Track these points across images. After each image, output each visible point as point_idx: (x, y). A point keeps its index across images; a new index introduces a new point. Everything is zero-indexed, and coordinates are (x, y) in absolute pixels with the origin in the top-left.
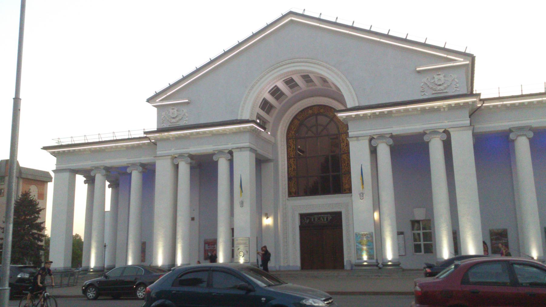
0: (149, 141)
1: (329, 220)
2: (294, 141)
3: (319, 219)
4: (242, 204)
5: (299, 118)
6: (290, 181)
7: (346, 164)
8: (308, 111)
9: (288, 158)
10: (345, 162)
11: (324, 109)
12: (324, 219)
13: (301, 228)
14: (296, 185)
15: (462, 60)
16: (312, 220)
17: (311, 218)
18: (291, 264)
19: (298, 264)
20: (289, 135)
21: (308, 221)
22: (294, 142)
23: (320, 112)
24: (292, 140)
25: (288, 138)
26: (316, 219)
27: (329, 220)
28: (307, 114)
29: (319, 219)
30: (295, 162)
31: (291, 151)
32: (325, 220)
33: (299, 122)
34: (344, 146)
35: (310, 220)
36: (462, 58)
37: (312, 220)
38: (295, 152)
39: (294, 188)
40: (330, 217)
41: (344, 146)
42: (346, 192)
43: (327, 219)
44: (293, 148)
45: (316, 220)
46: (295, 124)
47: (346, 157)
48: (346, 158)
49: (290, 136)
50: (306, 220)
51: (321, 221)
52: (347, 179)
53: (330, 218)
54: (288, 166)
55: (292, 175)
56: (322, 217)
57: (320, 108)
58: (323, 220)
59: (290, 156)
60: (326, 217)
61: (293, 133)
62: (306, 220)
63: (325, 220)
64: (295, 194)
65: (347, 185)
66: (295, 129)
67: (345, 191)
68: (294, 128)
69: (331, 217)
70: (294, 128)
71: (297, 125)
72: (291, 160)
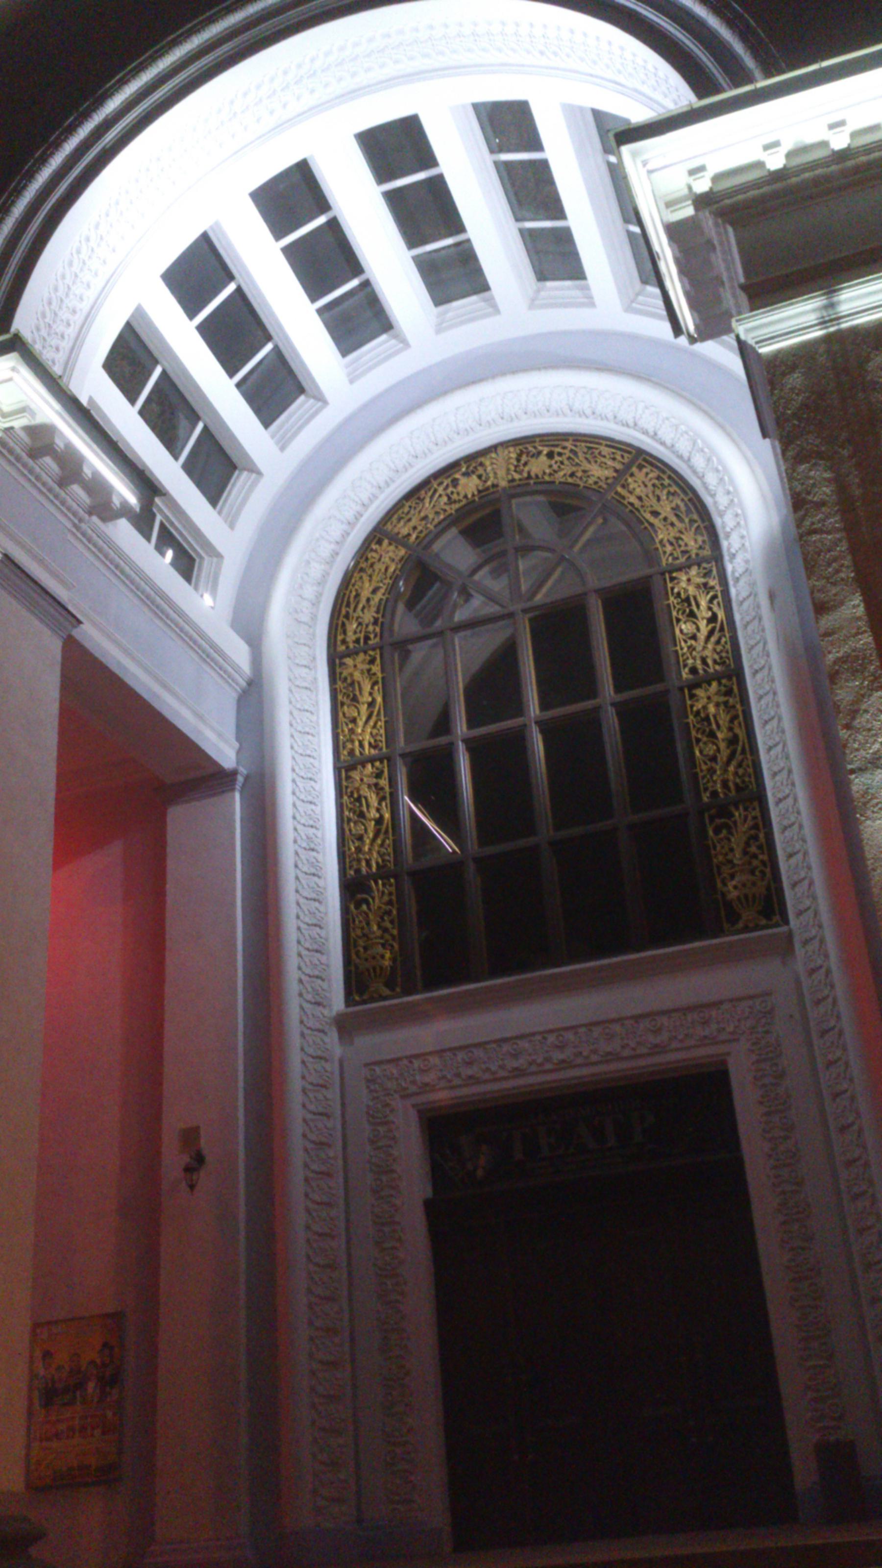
2: (372, 661)
5: (405, 531)
6: (358, 906)
7: (722, 745)
8: (455, 483)
9: (337, 770)
10: (712, 735)
11: (550, 455)
14: (392, 922)
20: (345, 632)
22: (376, 668)
23: (529, 477)
24: (362, 656)
25: (342, 648)
30: (384, 782)
31: (361, 723)
33: (402, 552)
41: (694, 637)
44: (371, 704)
47: (716, 699)
48: (717, 705)
49: (351, 637)
54: (340, 807)
55: (368, 862)
57: (524, 458)
59: (351, 753)
66: (379, 595)
68: (375, 591)
70: (375, 591)
71: (392, 569)
72: (356, 775)
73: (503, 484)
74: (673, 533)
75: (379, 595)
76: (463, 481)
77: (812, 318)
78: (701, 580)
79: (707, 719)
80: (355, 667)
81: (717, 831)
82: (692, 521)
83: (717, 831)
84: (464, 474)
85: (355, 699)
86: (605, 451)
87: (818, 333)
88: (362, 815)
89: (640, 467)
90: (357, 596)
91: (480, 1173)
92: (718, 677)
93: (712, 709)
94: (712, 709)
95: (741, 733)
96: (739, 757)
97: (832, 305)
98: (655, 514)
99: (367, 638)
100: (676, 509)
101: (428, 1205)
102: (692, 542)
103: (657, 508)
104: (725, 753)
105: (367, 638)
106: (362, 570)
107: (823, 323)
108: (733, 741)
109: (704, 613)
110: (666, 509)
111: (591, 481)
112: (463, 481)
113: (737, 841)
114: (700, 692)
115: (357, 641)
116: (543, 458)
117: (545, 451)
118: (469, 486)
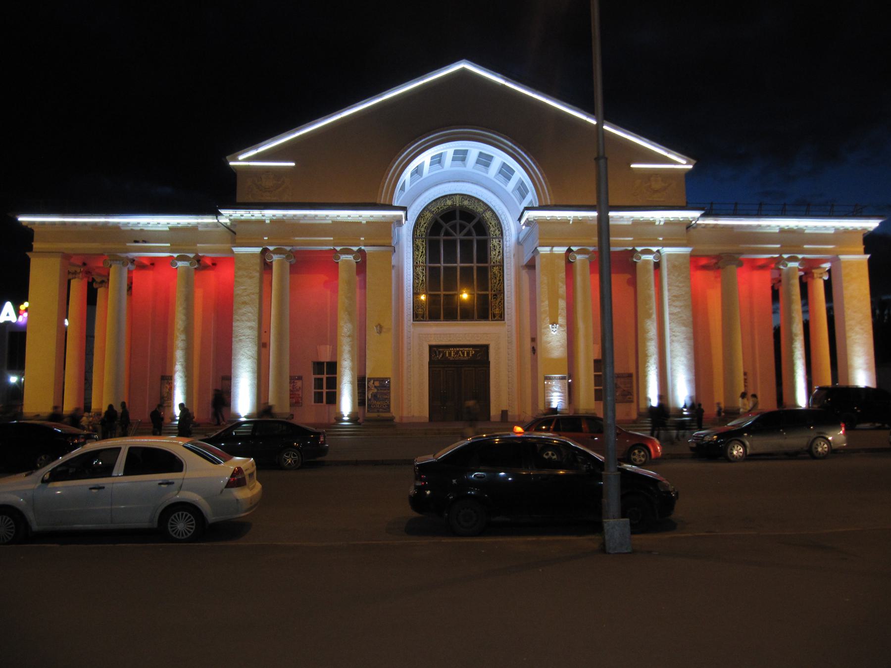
0: (216, 221)
1: (471, 355)
3: (457, 353)
4: (380, 329)
5: (433, 210)
7: (498, 281)
10: (496, 278)
11: (469, 201)
12: (463, 354)
13: (431, 362)
15: (684, 162)
16: (447, 355)
17: (446, 352)
18: (416, 414)
19: (426, 413)
21: (441, 356)
22: (424, 244)
26: (452, 354)
27: (471, 355)
28: (444, 206)
29: (457, 353)
30: (424, 272)
32: (465, 355)
34: (495, 255)
35: (444, 354)
36: (683, 158)
37: (447, 355)
38: (424, 257)
39: (422, 309)
40: (472, 352)
41: (495, 255)
42: (496, 318)
43: (468, 354)
45: (452, 356)
46: (426, 217)
49: (418, 234)
50: (438, 353)
51: (460, 356)
52: (499, 300)
53: (472, 352)
54: (413, 275)
56: (461, 351)
58: (462, 356)
59: (417, 263)
60: (467, 353)
61: (423, 230)
62: (438, 353)
63: (465, 355)
64: (423, 317)
65: (497, 309)
66: (425, 225)
67: (494, 317)
68: (425, 223)
69: (473, 352)
70: (425, 223)
71: (429, 219)
73: (458, 205)
74: (494, 229)
75: (425, 225)
76: (448, 201)
77: (549, 250)
78: (498, 243)
79: (495, 274)
80: (419, 242)
81: (494, 298)
82: (498, 228)
83: (494, 298)
84: (449, 199)
85: (418, 250)
86: (482, 204)
87: (549, 252)
88: (418, 278)
89: (489, 211)
90: (420, 223)
91: (440, 358)
92: (499, 266)
93: (496, 272)
94: (496, 272)
95: (502, 279)
96: (500, 284)
97: (552, 249)
98: (491, 223)
99: (422, 235)
100: (495, 223)
101: (429, 362)
102: (497, 232)
103: (491, 222)
104: (497, 283)
105: (422, 235)
106: (422, 217)
107: (550, 251)
108: (500, 280)
109: (497, 250)
110: (493, 224)
111: (478, 211)
112: (448, 201)
113: (498, 302)
114: (495, 268)
115: (420, 235)
116: (467, 201)
117: (468, 199)
118: (449, 203)
